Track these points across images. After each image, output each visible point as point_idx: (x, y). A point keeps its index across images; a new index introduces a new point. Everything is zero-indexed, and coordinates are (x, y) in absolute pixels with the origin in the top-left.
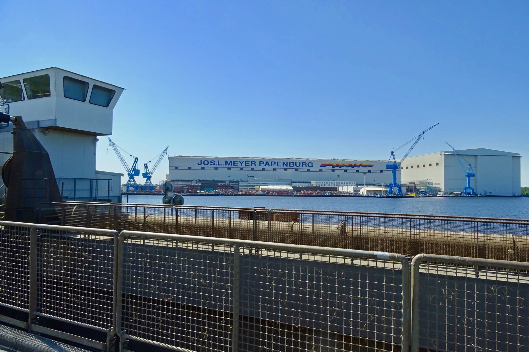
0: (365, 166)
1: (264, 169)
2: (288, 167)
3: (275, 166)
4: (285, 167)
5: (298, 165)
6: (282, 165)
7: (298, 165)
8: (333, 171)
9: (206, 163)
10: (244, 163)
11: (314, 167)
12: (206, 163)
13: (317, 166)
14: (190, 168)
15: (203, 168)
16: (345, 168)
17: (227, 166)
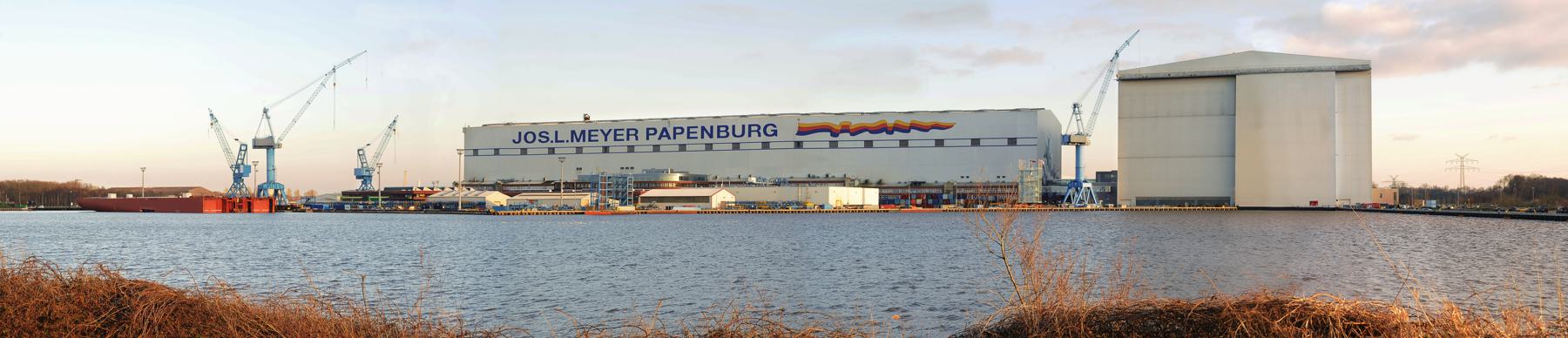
0: (924, 129)
1: (656, 148)
2: (715, 139)
4: (707, 139)
5: (738, 132)
7: (738, 132)
8: (834, 145)
9: (530, 138)
10: (611, 136)
12: (530, 138)
13: (788, 134)
14: (497, 152)
15: (524, 152)
16: (866, 136)
17: (576, 144)
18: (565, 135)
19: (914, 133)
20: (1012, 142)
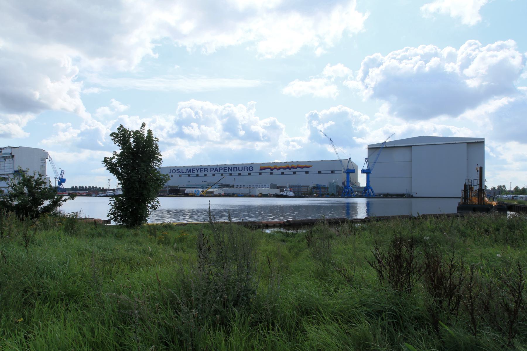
0: (302, 168)
1: (214, 175)
2: (233, 172)
3: (222, 172)
4: (230, 172)
5: (240, 169)
6: (227, 170)
7: (240, 169)
8: (271, 174)
9: (174, 171)
11: (254, 171)
12: (174, 171)
13: (257, 170)
16: (282, 170)
17: (188, 173)
18: (185, 171)
19: (298, 169)
20: (333, 172)
